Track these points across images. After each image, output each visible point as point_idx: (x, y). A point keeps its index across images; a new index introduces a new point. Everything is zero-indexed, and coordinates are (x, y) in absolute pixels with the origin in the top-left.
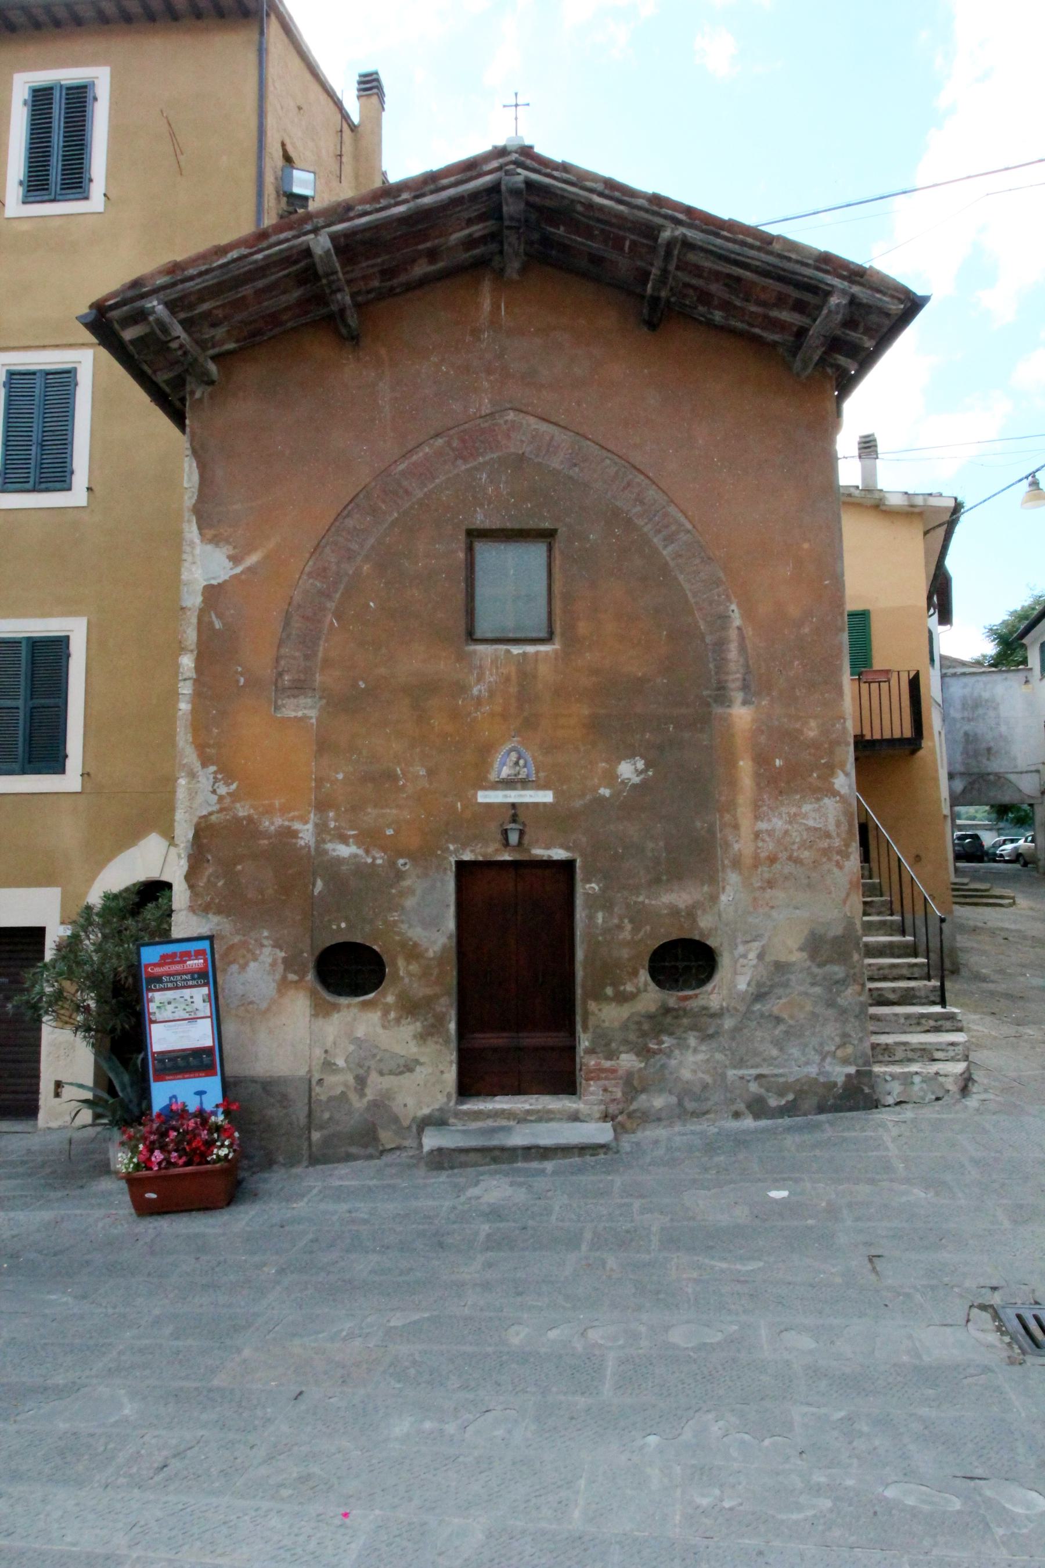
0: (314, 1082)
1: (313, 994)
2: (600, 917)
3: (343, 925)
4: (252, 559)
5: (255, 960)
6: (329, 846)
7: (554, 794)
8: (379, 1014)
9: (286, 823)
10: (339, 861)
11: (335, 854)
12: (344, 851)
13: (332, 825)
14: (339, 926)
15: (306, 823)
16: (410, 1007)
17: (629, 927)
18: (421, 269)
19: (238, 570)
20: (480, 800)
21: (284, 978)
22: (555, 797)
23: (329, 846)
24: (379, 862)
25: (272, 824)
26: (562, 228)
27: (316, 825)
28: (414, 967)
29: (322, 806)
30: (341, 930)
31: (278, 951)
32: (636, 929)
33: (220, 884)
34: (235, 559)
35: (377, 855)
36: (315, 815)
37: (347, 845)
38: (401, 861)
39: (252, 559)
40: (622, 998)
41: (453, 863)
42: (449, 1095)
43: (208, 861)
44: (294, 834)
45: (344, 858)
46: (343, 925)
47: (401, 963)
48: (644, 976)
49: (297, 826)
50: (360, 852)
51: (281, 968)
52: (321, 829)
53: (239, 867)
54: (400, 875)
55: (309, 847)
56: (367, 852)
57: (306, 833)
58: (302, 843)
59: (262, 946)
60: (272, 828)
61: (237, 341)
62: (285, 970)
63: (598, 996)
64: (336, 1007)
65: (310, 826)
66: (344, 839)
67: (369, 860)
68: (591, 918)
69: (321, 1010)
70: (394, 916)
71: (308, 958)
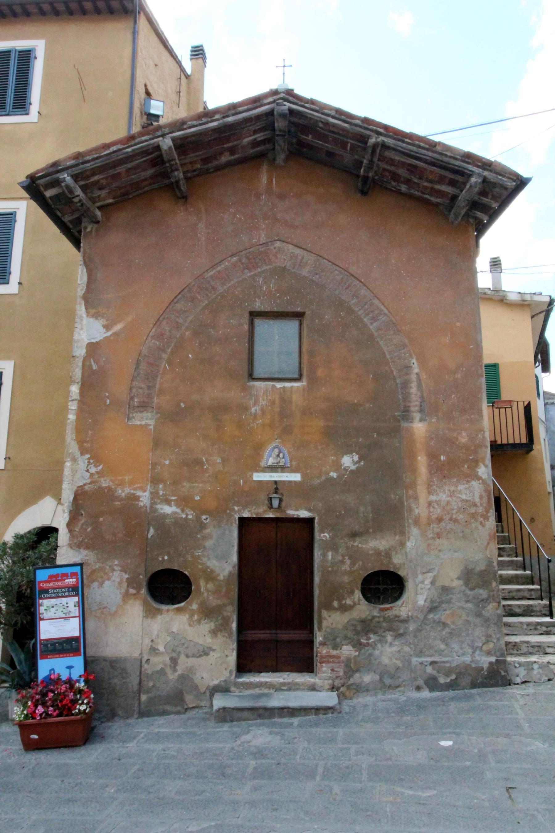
0: (144, 660)
1: (145, 603)
2: (330, 554)
3: (166, 558)
4: (118, 327)
5: (109, 579)
6: (159, 506)
7: (301, 475)
8: (187, 616)
9: (132, 491)
10: (165, 516)
11: (162, 511)
12: (168, 510)
13: (161, 493)
14: (163, 558)
15: (144, 491)
16: (207, 612)
17: (348, 562)
18: (225, 158)
19: (109, 334)
20: (255, 478)
21: (127, 591)
22: (302, 477)
23: (159, 506)
24: (190, 517)
25: (123, 492)
26: (310, 136)
27: (151, 493)
28: (210, 586)
29: (156, 480)
30: (164, 561)
31: (124, 574)
32: (353, 564)
33: (89, 529)
34: (107, 327)
35: (189, 513)
36: (151, 486)
37: (170, 506)
38: (204, 517)
39: (118, 327)
40: (344, 609)
41: (237, 519)
42: (231, 672)
43: (82, 515)
44: (137, 498)
45: (168, 515)
46: (166, 558)
47: (202, 583)
48: (358, 594)
49: (139, 493)
50: (178, 510)
51: (125, 585)
52: (154, 495)
53: (101, 519)
54: (203, 526)
55: (146, 507)
56: (183, 511)
57: (145, 498)
58: (142, 504)
59: (114, 570)
60: (123, 495)
61: (114, 198)
62: (128, 586)
63: (328, 606)
64: (159, 611)
65: (147, 494)
66: (168, 502)
67: (184, 516)
68: (324, 555)
69: (150, 613)
70: (198, 553)
71: (143, 579)
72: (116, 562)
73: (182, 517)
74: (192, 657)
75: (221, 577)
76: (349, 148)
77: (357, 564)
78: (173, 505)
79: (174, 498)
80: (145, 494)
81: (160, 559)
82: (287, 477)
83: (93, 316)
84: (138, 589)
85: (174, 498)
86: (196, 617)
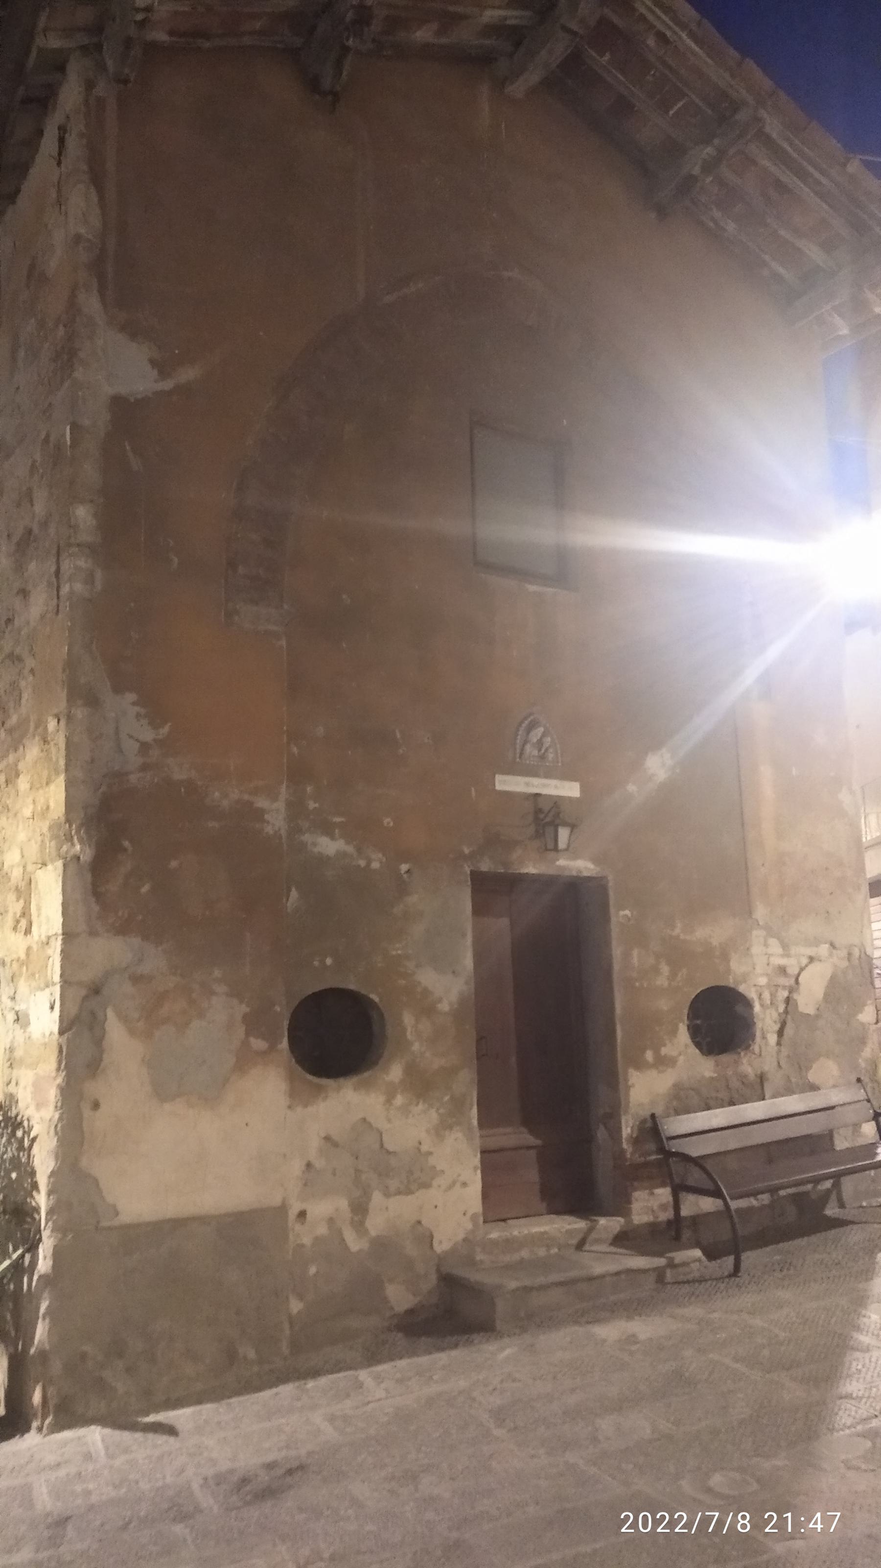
0: (293, 1213)
1: (291, 1078)
2: (635, 953)
3: (329, 961)
4: (188, 374)
5: (201, 1015)
6: (307, 838)
7: (581, 787)
8: (382, 1099)
9: (246, 797)
10: (323, 860)
11: (316, 850)
12: (329, 846)
13: (312, 805)
14: (323, 962)
15: (275, 799)
16: (420, 1085)
17: (665, 969)
18: (423, 35)
19: (167, 385)
20: (499, 787)
21: (245, 1044)
22: (582, 791)
23: (307, 838)
24: (375, 865)
25: (225, 796)
26: (607, 57)
27: (289, 804)
28: (426, 1026)
29: (298, 774)
31: (235, 1001)
32: (673, 975)
33: (145, 889)
34: (163, 368)
35: (373, 856)
36: (287, 787)
37: (333, 838)
38: (404, 867)
39: (188, 374)
40: (663, 1062)
41: (469, 872)
42: (474, 1218)
43: (125, 850)
44: (259, 815)
45: (328, 858)
46: (329, 961)
47: (408, 1019)
48: (683, 1035)
49: (261, 803)
50: (350, 849)
51: (241, 1031)
52: (296, 809)
53: (174, 864)
54: (402, 888)
55: (280, 837)
56: (359, 850)
57: (275, 817)
58: (269, 830)
59: (213, 993)
60: (225, 803)
61: (171, 33)
62: (248, 1034)
63: (640, 1065)
64: (320, 1088)
65: (280, 804)
66: (328, 829)
67: (362, 863)
68: (627, 955)
69: (298, 1096)
70: (396, 950)
71: (282, 1012)
72: (217, 973)
73: (359, 866)
74: (396, 1194)
75: (444, 1007)
76: (671, 112)
77: (680, 974)
78: (337, 836)
79: (338, 819)
80: (275, 805)
81: (316, 963)
82: (556, 787)
83: (123, 328)
84: (273, 1041)
85: (338, 819)
86: (399, 1100)
